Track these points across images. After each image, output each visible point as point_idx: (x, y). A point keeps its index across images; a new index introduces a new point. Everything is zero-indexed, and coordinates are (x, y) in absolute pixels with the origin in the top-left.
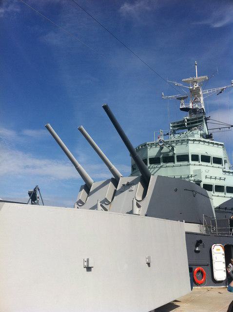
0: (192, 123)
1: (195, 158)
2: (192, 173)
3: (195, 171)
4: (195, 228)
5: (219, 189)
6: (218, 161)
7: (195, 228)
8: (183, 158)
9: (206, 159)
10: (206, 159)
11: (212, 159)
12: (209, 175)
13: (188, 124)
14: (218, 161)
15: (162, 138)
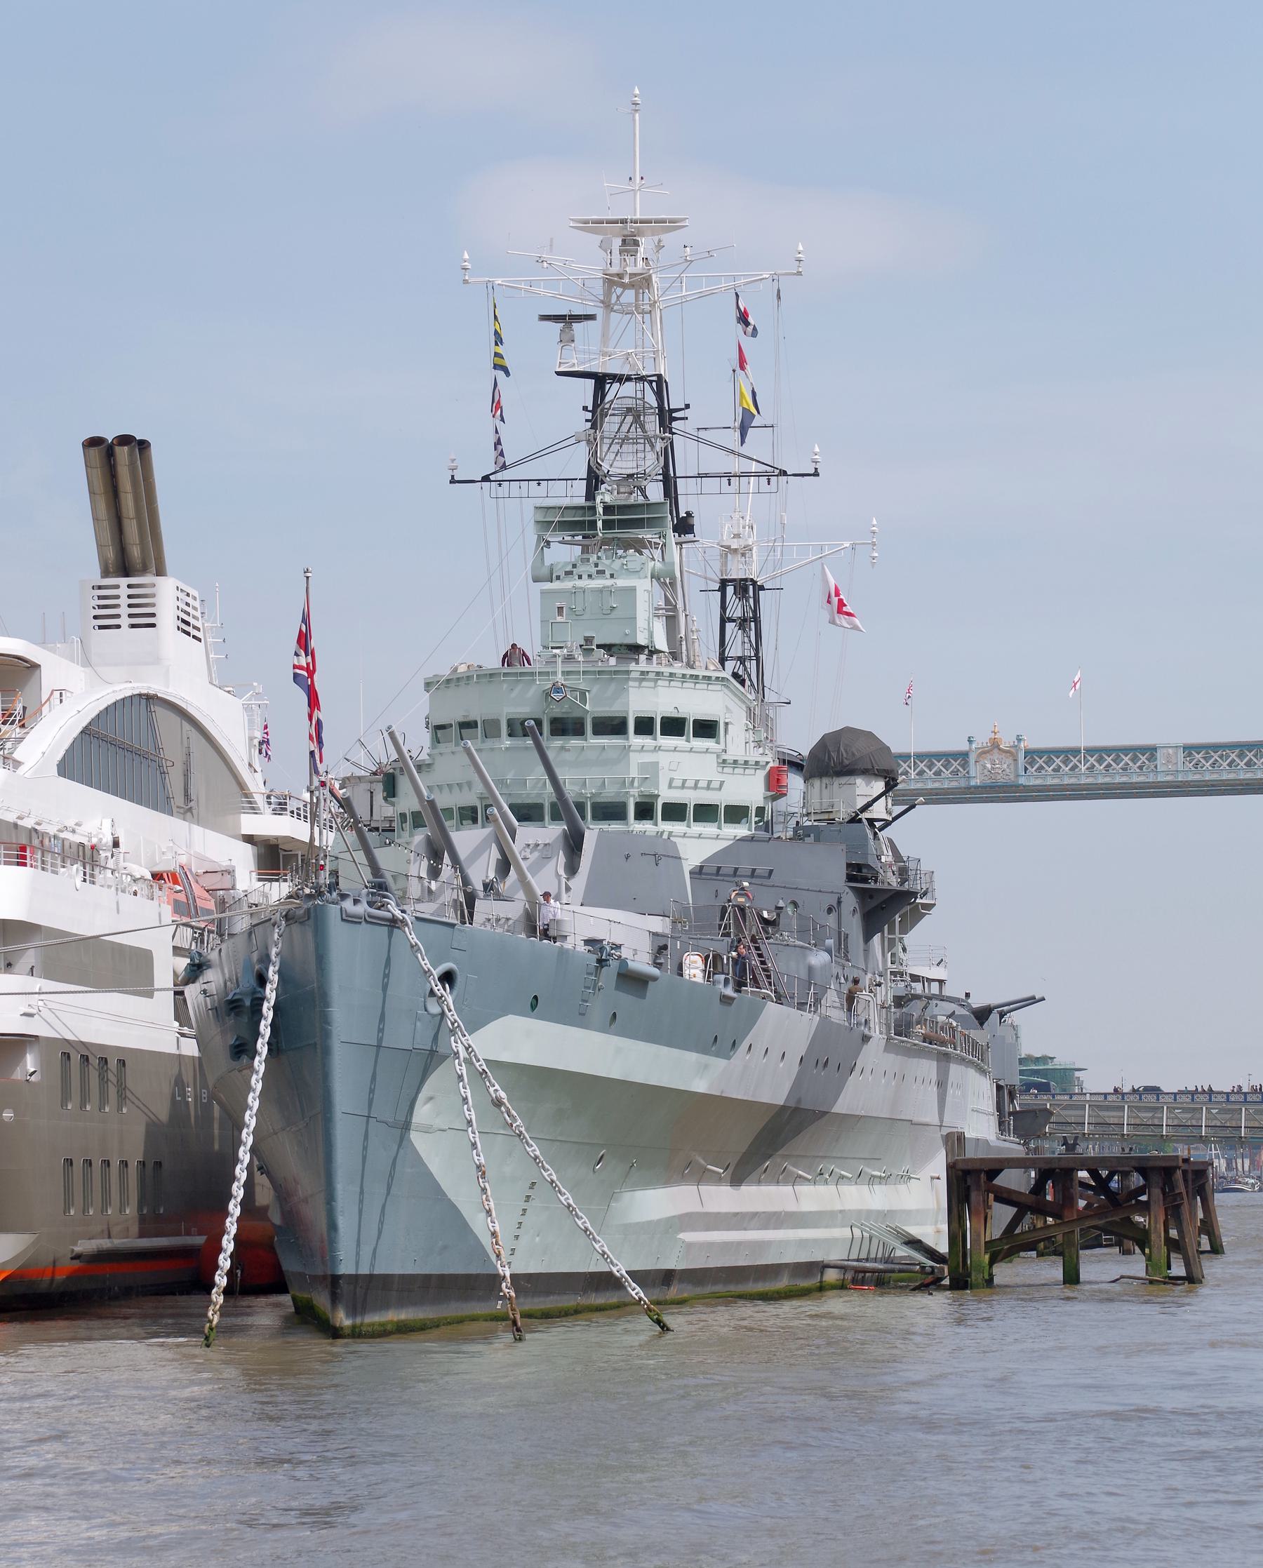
0: (624, 524)
1: (645, 726)
2: (634, 773)
3: (643, 767)
4: (659, 924)
5: (705, 813)
6: (706, 729)
7: (659, 924)
8: (613, 726)
9: (673, 726)
10: (673, 726)
11: (690, 728)
12: (678, 777)
13: (608, 525)
14: (706, 729)
15: (560, 678)
